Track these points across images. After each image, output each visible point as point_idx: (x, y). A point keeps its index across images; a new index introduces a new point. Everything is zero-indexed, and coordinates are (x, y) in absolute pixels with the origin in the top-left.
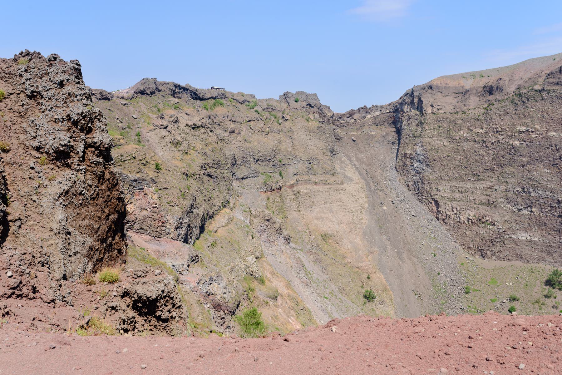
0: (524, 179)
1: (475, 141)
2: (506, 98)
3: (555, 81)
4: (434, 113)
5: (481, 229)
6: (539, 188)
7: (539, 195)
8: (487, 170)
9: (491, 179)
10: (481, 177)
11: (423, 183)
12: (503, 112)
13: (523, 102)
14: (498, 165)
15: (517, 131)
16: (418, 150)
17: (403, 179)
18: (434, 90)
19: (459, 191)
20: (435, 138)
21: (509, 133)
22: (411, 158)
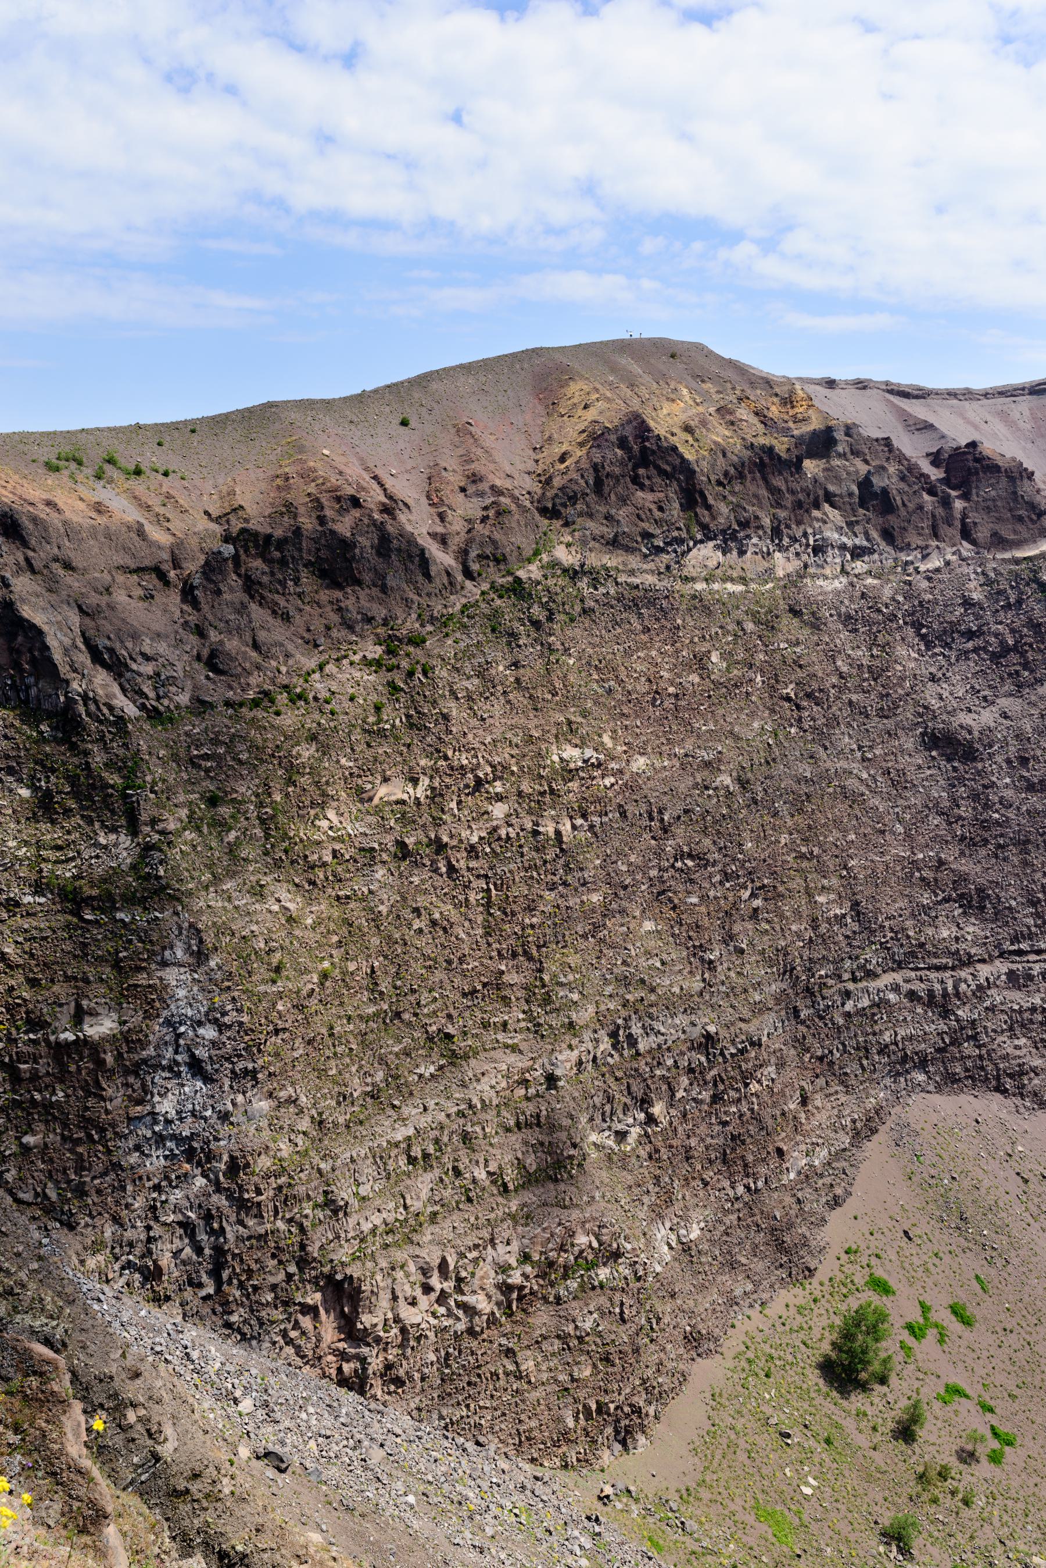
0: (609, 990)
1: (403, 851)
2: (458, 607)
3: (609, 532)
4: (154, 715)
5: (574, 1308)
6: (652, 1010)
7: (661, 1039)
8: (475, 991)
9: (500, 1036)
10: (461, 1044)
11: (242, 1205)
12: (476, 681)
13: (536, 624)
14: (514, 955)
15: (554, 771)
16: (181, 993)
17: (96, 1247)
18: (33, 542)
19: (412, 1160)
20: (228, 885)
21: (526, 787)
22: (135, 1070)
